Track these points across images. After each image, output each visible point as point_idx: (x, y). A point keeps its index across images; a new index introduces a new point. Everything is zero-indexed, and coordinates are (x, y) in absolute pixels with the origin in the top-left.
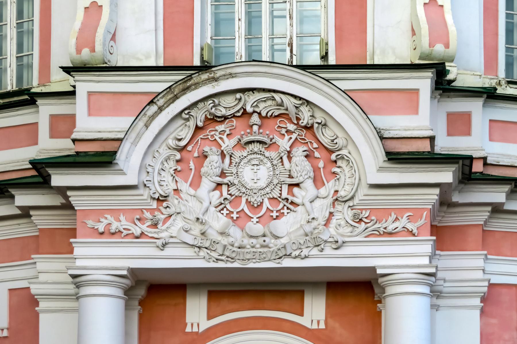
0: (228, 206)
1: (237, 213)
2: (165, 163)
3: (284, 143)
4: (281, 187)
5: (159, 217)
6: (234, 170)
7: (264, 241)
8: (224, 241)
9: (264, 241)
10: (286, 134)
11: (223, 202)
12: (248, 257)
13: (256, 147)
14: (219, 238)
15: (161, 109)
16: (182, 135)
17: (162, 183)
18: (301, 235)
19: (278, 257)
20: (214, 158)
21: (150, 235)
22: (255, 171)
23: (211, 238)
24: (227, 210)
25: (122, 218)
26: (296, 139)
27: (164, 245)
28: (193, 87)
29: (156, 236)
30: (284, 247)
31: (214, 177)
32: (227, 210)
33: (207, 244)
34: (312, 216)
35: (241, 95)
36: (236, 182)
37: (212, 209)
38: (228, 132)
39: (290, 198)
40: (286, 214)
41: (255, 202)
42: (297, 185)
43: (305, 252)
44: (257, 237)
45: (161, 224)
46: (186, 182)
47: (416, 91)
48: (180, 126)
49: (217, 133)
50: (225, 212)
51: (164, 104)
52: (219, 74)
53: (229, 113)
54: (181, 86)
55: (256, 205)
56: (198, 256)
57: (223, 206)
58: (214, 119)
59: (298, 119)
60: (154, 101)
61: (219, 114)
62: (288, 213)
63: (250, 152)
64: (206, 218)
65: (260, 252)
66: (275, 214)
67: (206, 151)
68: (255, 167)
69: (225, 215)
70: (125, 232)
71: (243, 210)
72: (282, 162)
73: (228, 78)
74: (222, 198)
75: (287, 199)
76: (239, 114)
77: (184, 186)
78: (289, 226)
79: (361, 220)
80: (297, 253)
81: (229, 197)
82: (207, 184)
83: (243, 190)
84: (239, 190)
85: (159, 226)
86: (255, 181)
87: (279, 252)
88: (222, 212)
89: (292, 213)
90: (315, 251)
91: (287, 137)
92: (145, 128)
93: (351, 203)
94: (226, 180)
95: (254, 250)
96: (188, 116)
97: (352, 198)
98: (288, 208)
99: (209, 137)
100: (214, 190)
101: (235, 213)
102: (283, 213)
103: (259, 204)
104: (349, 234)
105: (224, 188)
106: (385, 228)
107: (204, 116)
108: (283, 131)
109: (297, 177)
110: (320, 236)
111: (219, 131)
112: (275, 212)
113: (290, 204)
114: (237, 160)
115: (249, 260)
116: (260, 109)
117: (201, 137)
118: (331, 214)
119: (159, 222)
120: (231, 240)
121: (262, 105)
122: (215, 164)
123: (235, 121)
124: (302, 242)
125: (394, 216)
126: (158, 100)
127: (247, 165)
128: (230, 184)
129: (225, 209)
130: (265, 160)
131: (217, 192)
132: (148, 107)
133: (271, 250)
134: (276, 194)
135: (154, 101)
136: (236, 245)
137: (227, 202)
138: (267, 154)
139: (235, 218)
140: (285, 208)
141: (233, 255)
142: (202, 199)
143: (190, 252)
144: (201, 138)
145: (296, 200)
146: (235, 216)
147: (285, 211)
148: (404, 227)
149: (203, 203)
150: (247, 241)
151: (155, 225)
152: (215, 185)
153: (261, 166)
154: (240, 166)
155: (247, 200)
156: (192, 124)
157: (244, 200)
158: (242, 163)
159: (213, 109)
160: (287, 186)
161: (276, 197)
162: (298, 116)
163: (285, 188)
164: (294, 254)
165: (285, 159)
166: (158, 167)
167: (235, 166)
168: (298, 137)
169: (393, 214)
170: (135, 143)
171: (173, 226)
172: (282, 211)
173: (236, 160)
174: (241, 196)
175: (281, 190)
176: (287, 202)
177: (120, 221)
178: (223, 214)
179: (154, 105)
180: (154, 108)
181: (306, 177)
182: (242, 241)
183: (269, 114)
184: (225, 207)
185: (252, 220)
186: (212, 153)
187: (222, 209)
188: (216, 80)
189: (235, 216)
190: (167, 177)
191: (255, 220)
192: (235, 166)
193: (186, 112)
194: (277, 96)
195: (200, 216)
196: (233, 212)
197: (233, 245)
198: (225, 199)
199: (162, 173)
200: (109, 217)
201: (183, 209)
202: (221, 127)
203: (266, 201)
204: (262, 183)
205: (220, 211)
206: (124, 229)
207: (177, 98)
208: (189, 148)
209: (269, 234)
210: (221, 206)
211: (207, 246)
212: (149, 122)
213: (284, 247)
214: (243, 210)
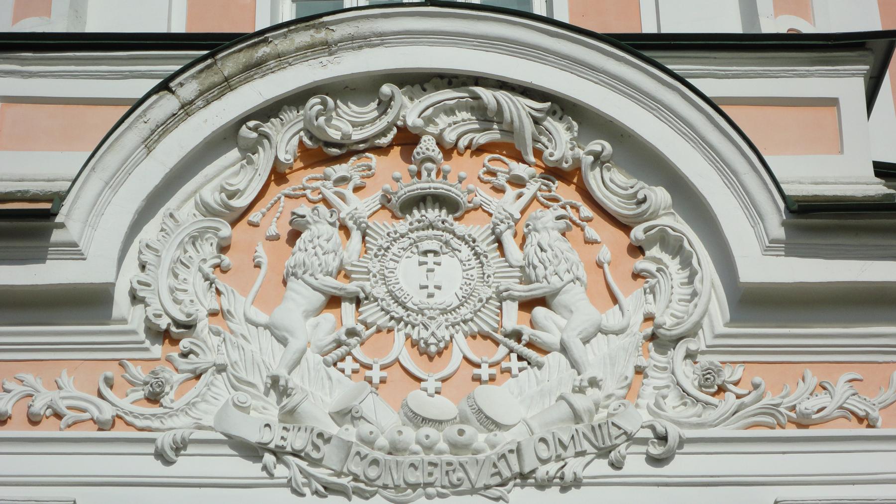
0: (357, 352)
1: (383, 368)
2: (190, 248)
3: (509, 203)
4: (500, 308)
5: (167, 375)
6: (375, 266)
7: (461, 432)
8: (350, 433)
9: (461, 432)
10: (508, 186)
11: (344, 337)
12: (412, 480)
13: (433, 214)
14: (331, 428)
15: (187, 108)
16: (238, 182)
17: (180, 296)
18: (562, 421)
19: (497, 480)
20: (320, 230)
21: (139, 423)
22: (431, 265)
23: (310, 424)
24: (355, 360)
25: (65, 379)
26: (535, 197)
27: (179, 447)
28: (272, 63)
29: (156, 424)
30: (518, 451)
31: (320, 276)
32: (355, 360)
33: (297, 441)
34: (587, 375)
35: (395, 88)
36: (380, 291)
37: (313, 358)
38: (356, 180)
39: (528, 332)
40: (515, 371)
41: (432, 340)
42: (543, 301)
43: (574, 466)
44: (441, 422)
45: (172, 395)
46: (245, 293)
47: (833, 102)
48: (233, 165)
49: (329, 184)
50: (349, 364)
51: (197, 97)
52: (340, 31)
53: (357, 135)
54: (242, 55)
55: (433, 349)
56: (271, 476)
57: (343, 349)
58: (320, 152)
59: (538, 153)
60: (172, 85)
61: (335, 135)
62: (521, 370)
63: (416, 224)
64: (295, 380)
65: (449, 464)
66: (485, 372)
67: (301, 213)
68: (431, 258)
69: (348, 371)
70: (71, 416)
71: (397, 360)
72: (501, 247)
73: (360, 47)
74: (343, 330)
75: (517, 335)
76: (384, 141)
77: (238, 303)
78: (524, 403)
79: (722, 389)
80: (552, 468)
81: (360, 327)
82: (302, 296)
83: (400, 312)
84: (388, 312)
85: (165, 401)
86: (431, 290)
87: (502, 465)
88: (340, 365)
89: (531, 371)
90: (601, 467)
91: (511, 192)
92: (142, 150)
93: (692, 345)
94: (352, 287)
95: (432, 457)
96: (254, 135)
97: (692, 333)
98: (520, 358)
99: (308, 192)
100: (318, 312)
101: (376, 367)
102: (508, 370)
103: (442, 345)
104: (695, 420)
105: (347, 308)
106: (793, 408)
107: (295, 141)
108: (502, 180)
109: (545, 277)
110: (616, 420)
111: (335, 176)
112: (485, 366)
113: (524, 346)
114: (380, 242)
115: (414, 487)
116: (441, 126)
117: (286, 191)
118: (640, 371)
119: (167, 389)
120: (365, 428)
121: (443, 121)
122: (324, 244)
123: (373, 159)
124: (566, 439)
125: (812, 380)
126: (181, 85)
127: (409, 253)
128: (362, 295)
129: (349, 359)
130: (455, 243)
131: (329, 316)
132: (154, 98)
133: (481, 457)
134: (486, 321)
135: (172, 85)
136: (382, 441)
137: (353, 341)
138: (460, 228)
139: (376, 380)
140: (514, 356)
141: (373, 473)
142: (287, 331)
143: (250, 469)
144: (287, 196)
145: (542, 336)
146: (376, 374)
147: (514, 364)
148: (841, 407)
149: (290, 339)
150: (410, 434)
151: (154, 398)
152: (321, 299)
153: (442, 258)
154: (390, 255)
155: (408, 336)
156: (263, 161)
157: (399, 337)
158: (394, 249)
159: (322, 119)
160: (516, 305)
161: (486, 328)
162: (539, 146)
163: (511, 309)
164: (542, 471)
165: (509, 240)
166: (169, 254)
167: (376, 256)
168: (539, 194)
169: (809, 374)
170: (114, 183)
171: (204, 401)
172: (504, 365)
173: (377, 241)
174: (390, 330)
175: (501, 315)
176: (519, 340)
177: (60, 388)
178: (343, 371)
179: (169, 96)
180: (167, 104)
181: (567, 277)
182: (400, 432)
183: (463, 143)
184: (349, 354)
185: (423, 384)
186: (316, 218)
187: (342, 359)
188: (328, 47)
189: (376, 374)
190: (194, 282)
191: (431, 384)
192: (376, 256)
193: (252, 124)
194: (487, 95)
195: (283, 372)
196: (369, 367)
197: (370, 443)
198: (351, 333)
199: (182, 272)
200: (29, 378)
201: (235, 356)
202: (340, 170)
203: (460, 337)
204: (447, 297)
205: (335, 364)
206: (69, 408)
207: (231, 89)
208: (254, 216)
209: (473, 418)
210: (337, 352)
211: (298, 446)
212: (155, 137)
213: (518, 451)
214: (397, 360)
